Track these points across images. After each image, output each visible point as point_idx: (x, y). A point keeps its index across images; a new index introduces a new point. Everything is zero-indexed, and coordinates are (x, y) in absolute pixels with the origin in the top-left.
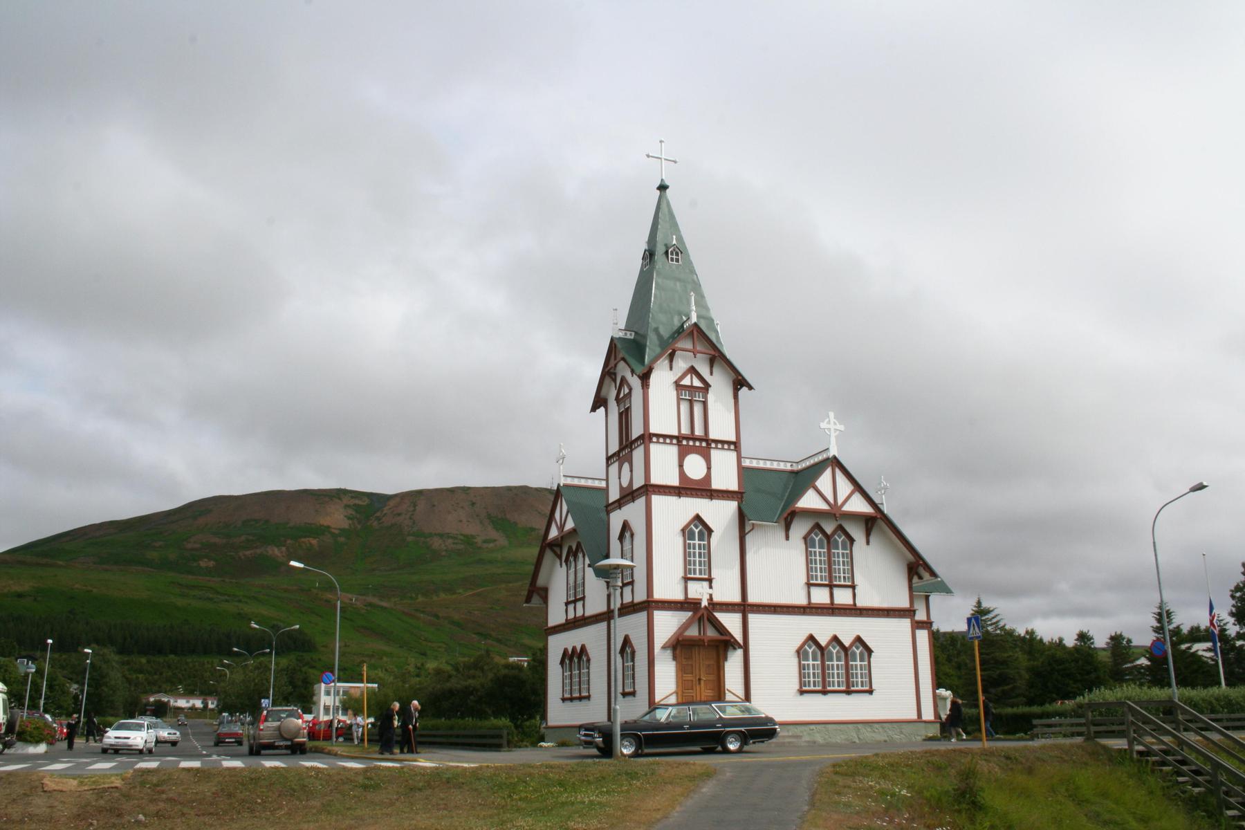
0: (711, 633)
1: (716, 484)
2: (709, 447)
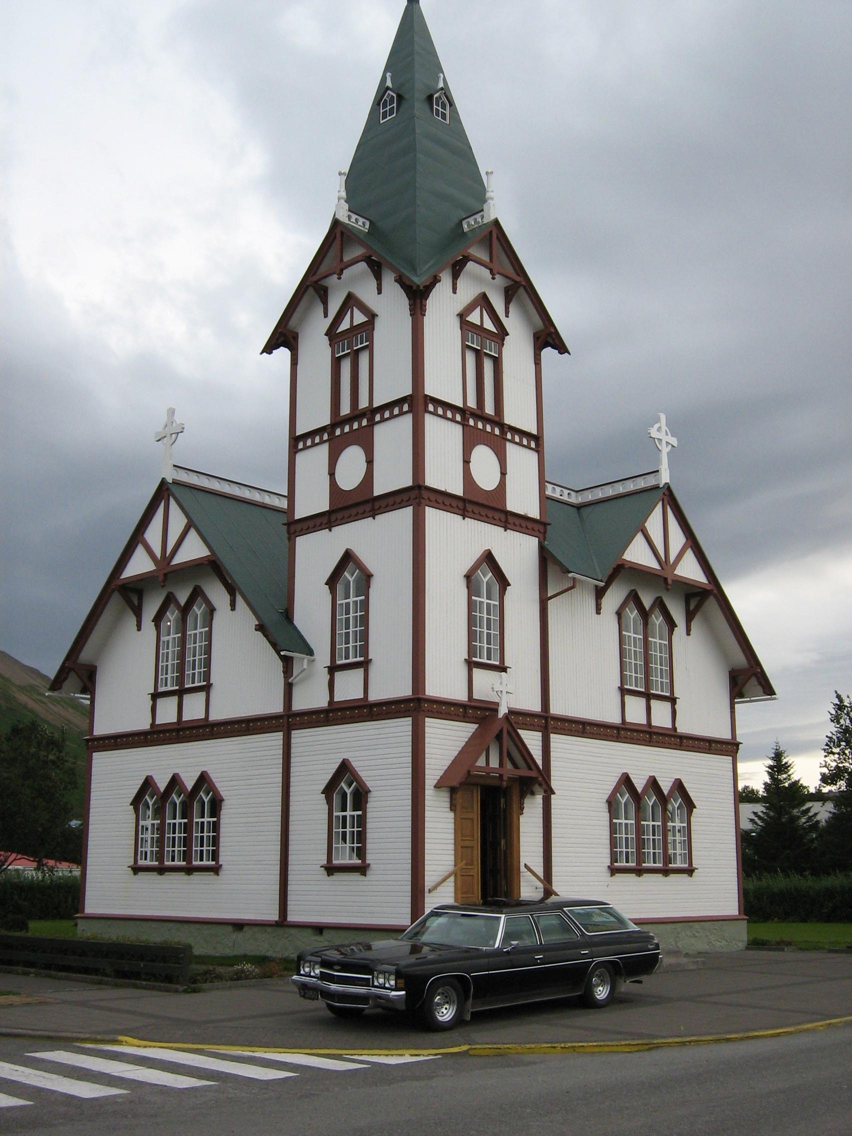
1: (513, 504)
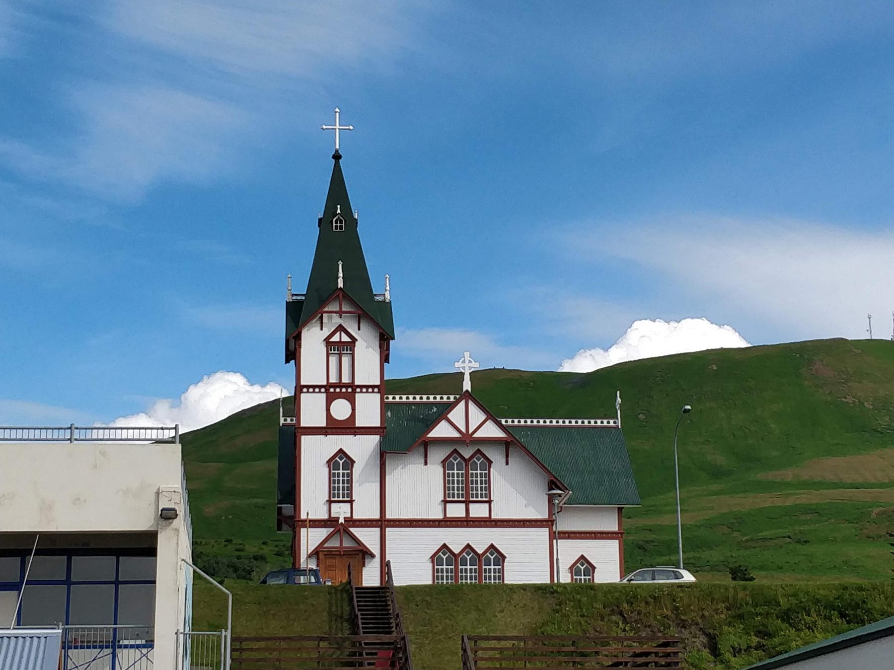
0: (347, 544)
2: (354, 392)
